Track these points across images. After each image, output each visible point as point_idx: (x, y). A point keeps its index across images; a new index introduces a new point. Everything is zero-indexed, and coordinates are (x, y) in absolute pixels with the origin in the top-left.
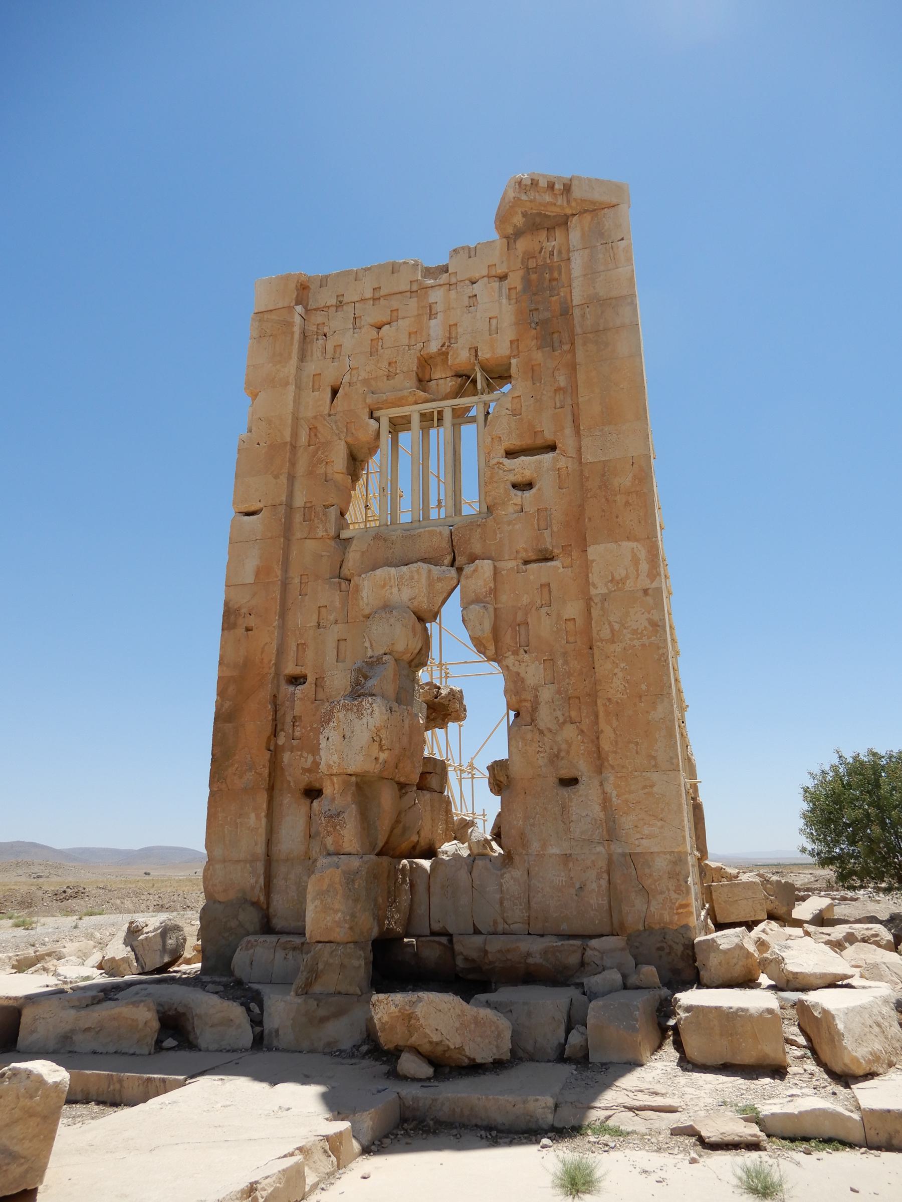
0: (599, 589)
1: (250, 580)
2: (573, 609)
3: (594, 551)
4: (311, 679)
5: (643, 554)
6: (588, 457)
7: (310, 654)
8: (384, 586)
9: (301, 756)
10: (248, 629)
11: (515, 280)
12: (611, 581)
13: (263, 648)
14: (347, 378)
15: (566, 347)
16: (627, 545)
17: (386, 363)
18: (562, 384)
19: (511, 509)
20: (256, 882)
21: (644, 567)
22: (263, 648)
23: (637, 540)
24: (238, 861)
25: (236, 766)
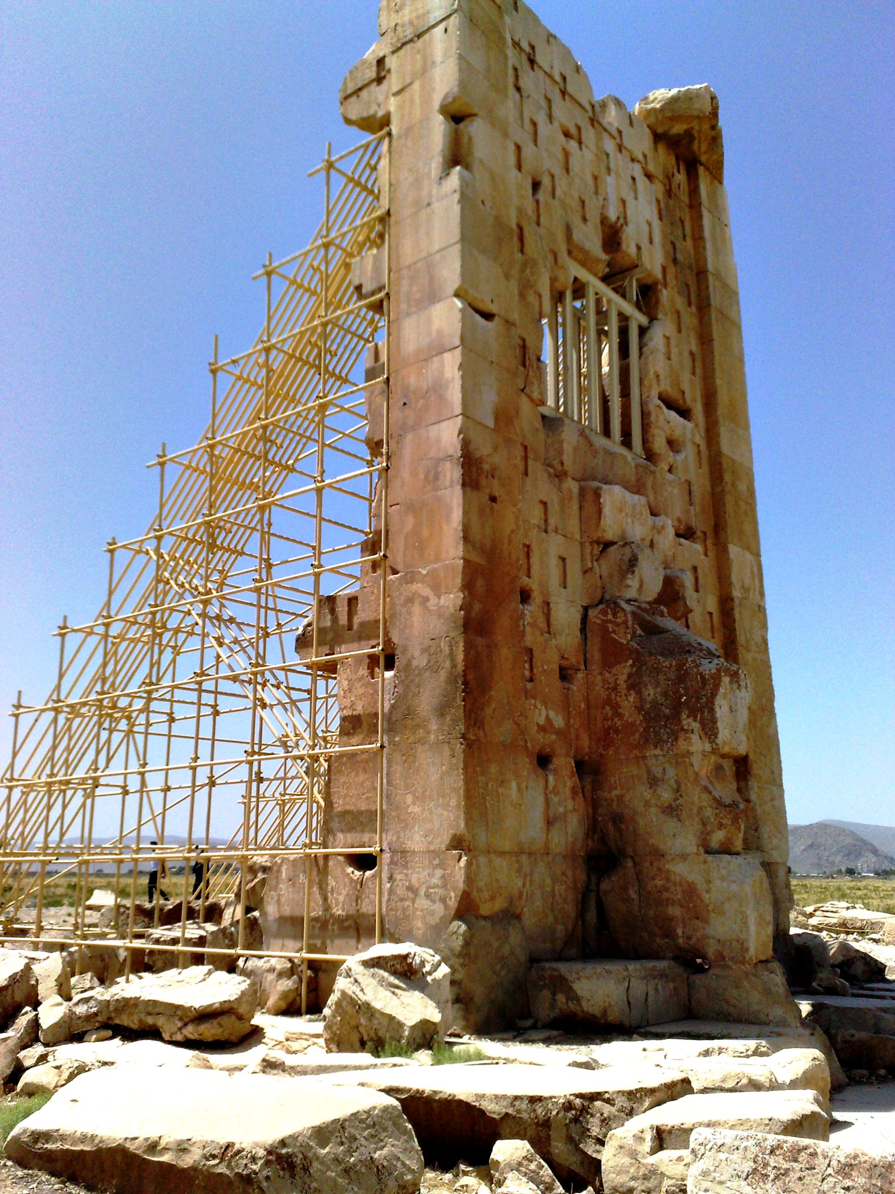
0: (736, 593)
1: (490, 423)
2: (712, 604)
3: (734, 550)
4: (537, 597)
5: (755, 569)
6: (725, 446)
7: (535, 560)
8: (621, 510)
9: (535, 707)
10: (493, 499)
11: (658, 188)
12: (743, 587)
13: (510, 537)
14: (546, 181)
15: (694, 309)
16: (748, 556)
17: (576, 195)
18: (694, 348)
19: (666, 468)
20: (524, 885)
21: (757, 581)
22: (510, 537)
23: (752, 553)
24: (502, 854)
25: (493, 706)
